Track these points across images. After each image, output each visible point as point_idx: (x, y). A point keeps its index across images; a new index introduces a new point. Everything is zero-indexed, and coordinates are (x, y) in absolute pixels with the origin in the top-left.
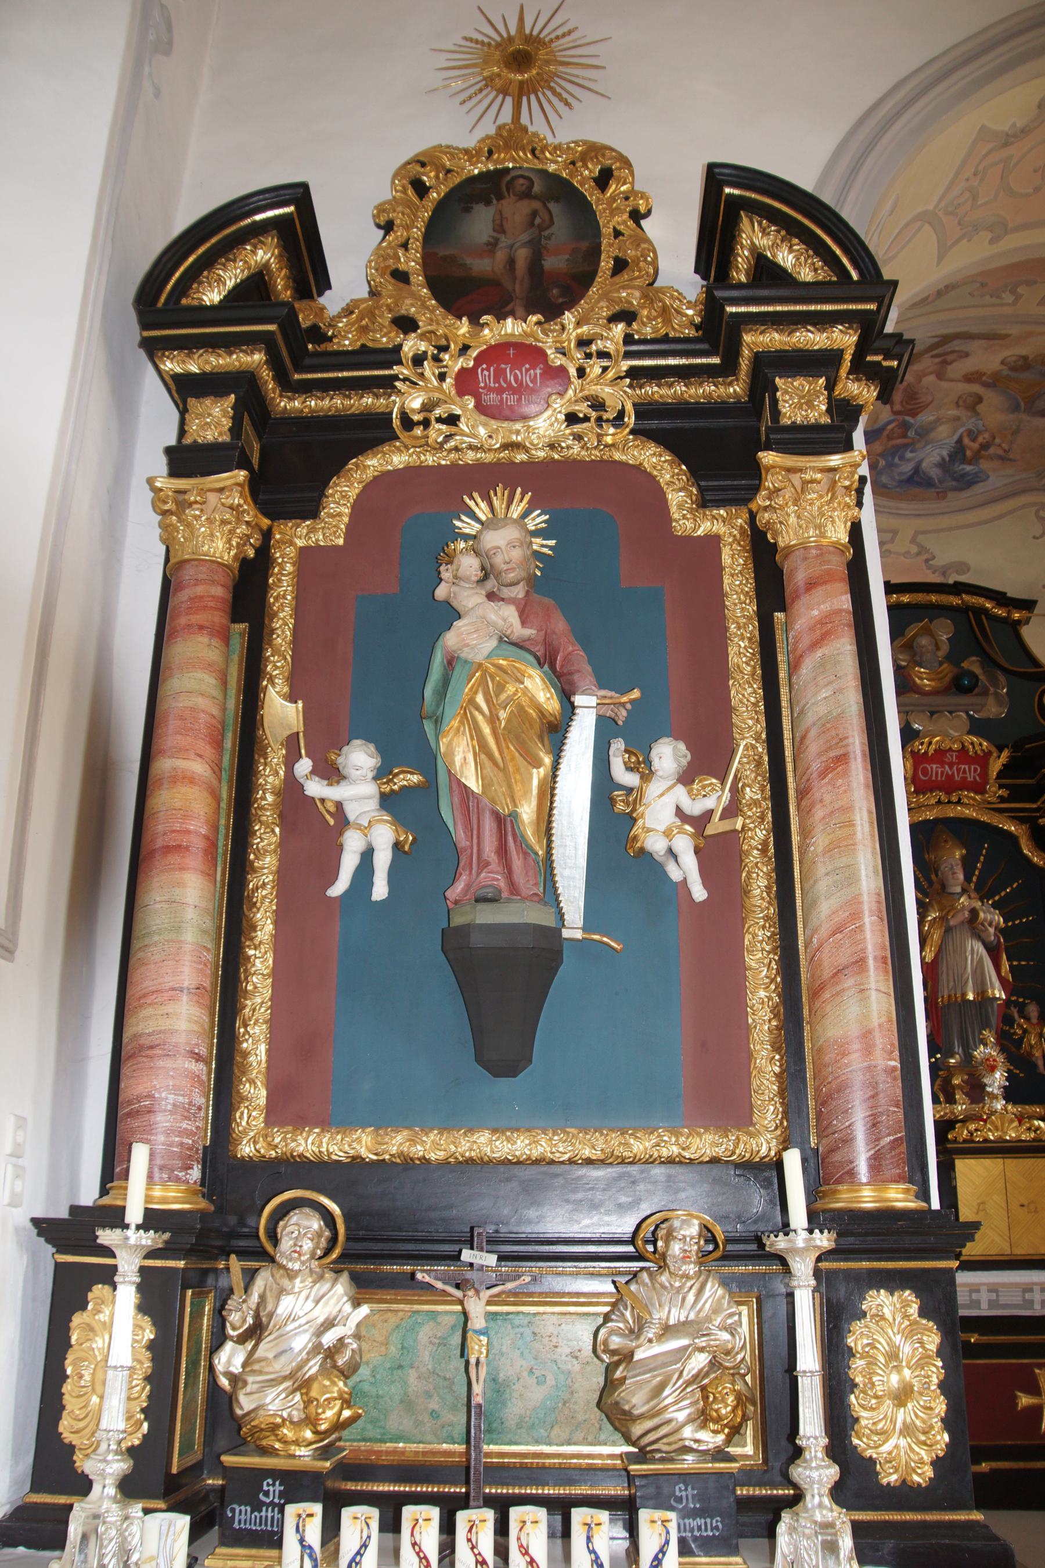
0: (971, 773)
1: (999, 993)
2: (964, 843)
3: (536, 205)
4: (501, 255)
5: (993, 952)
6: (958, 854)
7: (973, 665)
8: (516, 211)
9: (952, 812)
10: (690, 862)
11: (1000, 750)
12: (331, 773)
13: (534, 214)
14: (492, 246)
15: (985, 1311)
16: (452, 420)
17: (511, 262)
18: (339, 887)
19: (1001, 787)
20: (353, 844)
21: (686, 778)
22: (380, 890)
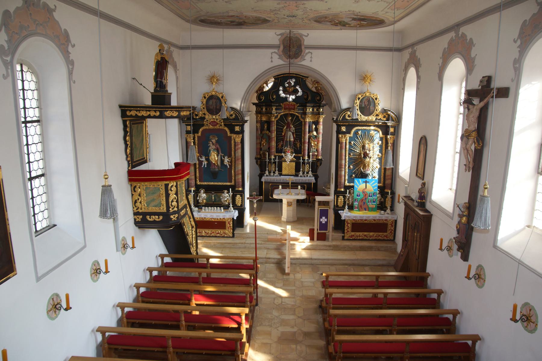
0: (293, 107)
1: (292, 140)
3: (216, 100)
4: (213, 106)
5: (293, 133)
6: (290, 118)
7: (298, 87)
8: (214, 101)
9: (291, 112)
10: (228, 165)
11: (297, 104)
12: (201, 157)
13: (216, 101)
14: (212, 105)
15: (282, 182)
16: (209, 126)
17: (214, 107)
18: (203, 167)
20: (203, 163)
22: (206, 166)
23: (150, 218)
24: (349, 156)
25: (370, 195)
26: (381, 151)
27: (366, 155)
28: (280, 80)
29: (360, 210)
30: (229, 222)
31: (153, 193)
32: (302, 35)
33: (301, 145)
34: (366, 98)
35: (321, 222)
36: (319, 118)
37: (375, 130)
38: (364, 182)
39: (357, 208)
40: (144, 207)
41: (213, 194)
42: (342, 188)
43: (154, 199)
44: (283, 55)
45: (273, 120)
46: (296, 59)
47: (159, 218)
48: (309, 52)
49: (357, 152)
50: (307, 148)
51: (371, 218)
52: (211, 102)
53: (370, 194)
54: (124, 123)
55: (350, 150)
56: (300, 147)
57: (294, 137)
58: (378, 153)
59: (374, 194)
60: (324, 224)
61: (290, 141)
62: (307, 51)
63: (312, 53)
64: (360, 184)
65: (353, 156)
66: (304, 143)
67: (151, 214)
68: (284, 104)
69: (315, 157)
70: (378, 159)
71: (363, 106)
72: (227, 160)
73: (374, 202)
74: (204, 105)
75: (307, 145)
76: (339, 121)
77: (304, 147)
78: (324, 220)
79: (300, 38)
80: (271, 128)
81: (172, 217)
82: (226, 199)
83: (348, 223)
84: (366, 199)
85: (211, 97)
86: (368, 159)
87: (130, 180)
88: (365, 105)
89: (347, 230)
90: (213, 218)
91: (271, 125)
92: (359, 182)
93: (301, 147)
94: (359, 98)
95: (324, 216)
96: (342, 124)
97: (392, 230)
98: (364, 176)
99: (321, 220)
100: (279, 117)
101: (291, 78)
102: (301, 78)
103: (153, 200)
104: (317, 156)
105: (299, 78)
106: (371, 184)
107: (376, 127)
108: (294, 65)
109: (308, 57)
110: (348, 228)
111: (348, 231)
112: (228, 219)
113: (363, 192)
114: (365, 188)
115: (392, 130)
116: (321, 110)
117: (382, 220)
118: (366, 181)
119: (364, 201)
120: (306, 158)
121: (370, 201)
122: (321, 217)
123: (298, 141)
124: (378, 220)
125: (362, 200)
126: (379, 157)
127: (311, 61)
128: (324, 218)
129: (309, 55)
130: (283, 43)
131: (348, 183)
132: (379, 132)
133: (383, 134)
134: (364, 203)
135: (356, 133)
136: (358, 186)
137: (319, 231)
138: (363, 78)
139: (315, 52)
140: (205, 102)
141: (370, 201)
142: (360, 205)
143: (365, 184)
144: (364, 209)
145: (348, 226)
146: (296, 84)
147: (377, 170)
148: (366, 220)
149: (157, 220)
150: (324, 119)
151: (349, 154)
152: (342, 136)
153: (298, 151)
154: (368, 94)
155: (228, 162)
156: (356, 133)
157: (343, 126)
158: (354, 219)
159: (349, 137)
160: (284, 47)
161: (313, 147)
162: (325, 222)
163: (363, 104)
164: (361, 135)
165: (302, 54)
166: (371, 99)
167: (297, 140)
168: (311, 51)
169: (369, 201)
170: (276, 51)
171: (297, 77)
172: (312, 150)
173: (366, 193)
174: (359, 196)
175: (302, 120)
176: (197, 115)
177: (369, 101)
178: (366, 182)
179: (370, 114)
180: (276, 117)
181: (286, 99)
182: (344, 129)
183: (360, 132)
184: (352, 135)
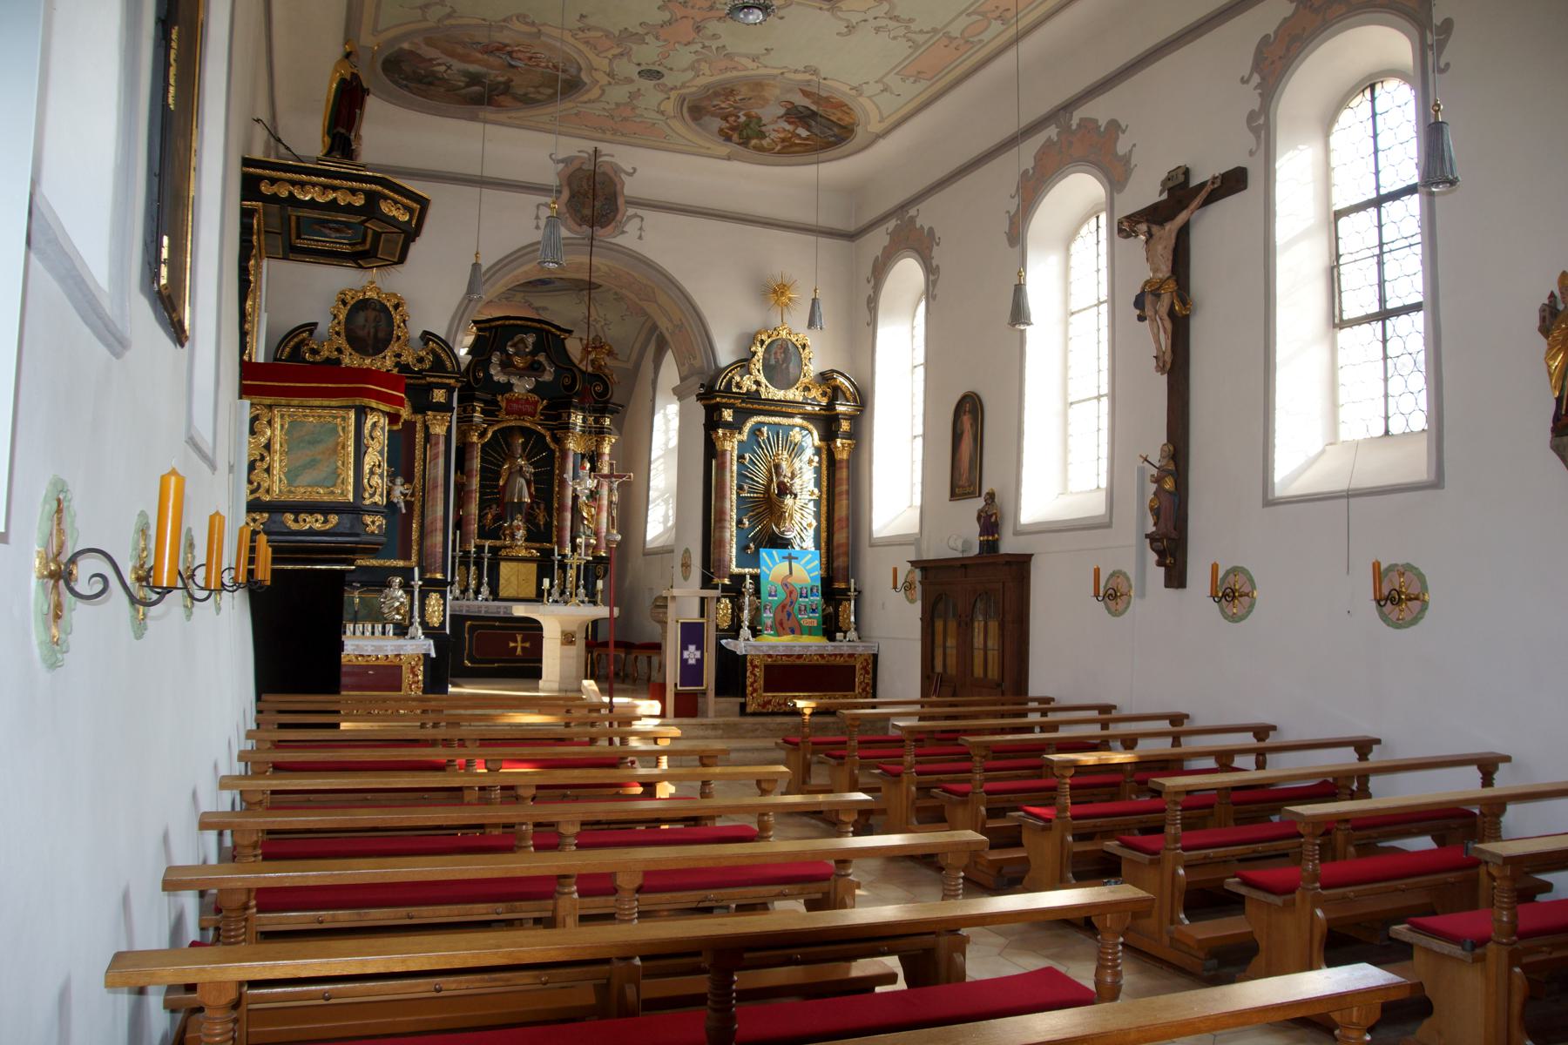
0: (530, 408)
1: (527, 500)
2: (523, 436)
4: (366, 330)
5: (528, 483)
6: (520, 441)
7: (541, 358)
8: (372, 314)
10: (402, 505)
11: (543, 400)
15: (502, 615)
17: (369, 333)
19: (542, 414)
21: (403, 485)
23: (296, 521)
24: (737, 493)
25: (801, 593)
26: (818, 483)
27: (784, 490)
28: (492, 336)
29: (778, 634)
30: (413, 668)
31: (313, 443)
32: (617, 170)
33: (551, 516)
34: (780, 342)
35: (684, 662)
36: (599, 443)
37: (802, 428)
38: (784, 558)
39: (771, 628)
40: (277, 487)
41: (358, 588)
42: (724, 577)
43: (313, 460)
44: (567, 215)
45: (475, 439)
46: (602, 228)
47: (326, 521)
48: (636, 216)
49: (758, 482)
50: (568, 523)
51: (812, 651)
52: (361, 318)
53: (801, 589)
54: (246, 214)
55: (741, 476)
56: (549, 525)
57: (530, 494)
58: (811, 486)
59: (812, 590)
60: (692, 665)
61: (521, 503)
62: (631, 211)
63: (642, 219)
64: (775, 563)
65: (750, 492)
66: (562, 508)
67: (298, 508)
68: (507, 399)
69: (590, 552)
70: (812, 503)
71: (773, 362)
72: (401, 489)
73: (814, 611)
74: (339, 323)
75: (568, 515)
76: (719, 391)
77: (561, 520)
78: (692, 654)
79: (612, 174)
80: (467, 464)
81: (368, 519)
82: (397, 604)
83: (754, 667)
84: (792, 603)
85: (363, 305)
86: (789, 500)
87: (245, 391)
88: (777, 362)
89: (752, 685)
90: (362, 656)
91: (467, 456)
92: (771, 557)
93: (552, 522)
94: (762, 342)
95: (692, 644)
96: (724, 401)
97: (867, 684)
98: (780, 542)
99: (686, 655)
100: (490, 435)
101: (526, 330)
102: (553, 334)
103: (312, 464)
104: (596, 548)
105: (548, 332)
106: (803, 562)
107: (803, 418)
108: (602, 244)
109: (632, 227)
110: (755, 681)
111: (755, 690)
112: (411, 657)
113: (785, 585)
114: (788, 573)
115: (845, 426)
116: (608, 422)
117: (842, 655)
118: (790, 554)
119: (788, 608)
120: (568, 551)
121: (803, 608)
122: (684, 647)
123: (542, 506)
124: (830, 655)
125: (784, 607)
126: (814, 497)
127: (640, 237)
128: (692, 648)
129: (635, 223)
130: (569, 185)
131: (737, 566)
132: (810, 433)
133: (820, 440)
134: (789, 615)
135: (756, 431)
136: (770, 569)
137: (679, 688)
138: (774, 292)
139: (649, 215)
140: (342, 317)
141: (803, 608)
142: (779, 618)
143: (787, 563)
144: (789, 631)
145: (755, 675)
146: (538, 347)
147: (811, 532)
148: (800, 656)
149: (317, 526)
150: (613, 447)
151: (740, 488)
152: (724, 434)
153: (541, 534)
154: (784, 334)
155: (405, 495)
156: (756, 431)
157: (726, 408)
158: (771, 653)
159: (739, 442)
160: (572, 196)
161: (586, 522)
162: (697, 660)
163: (773, 356)
164: (768, 438)
165: (619, 217)
166: (790, 346)
167: (538, 504)
168: (640, 212)
169: (800, 610)
170: (548, 200)
171: (542, 330)
172: (582, 530)
173: (791, 588)
174: (775, 596)
175: (552, 446)
176: (314, 352)
177: (785, 350)
178: (790, 558)
179: (788, 385)
180: (482, 435)
181: (509, 387)
182: (728, 415)
183: (765, 429)
184: (744, 437)
